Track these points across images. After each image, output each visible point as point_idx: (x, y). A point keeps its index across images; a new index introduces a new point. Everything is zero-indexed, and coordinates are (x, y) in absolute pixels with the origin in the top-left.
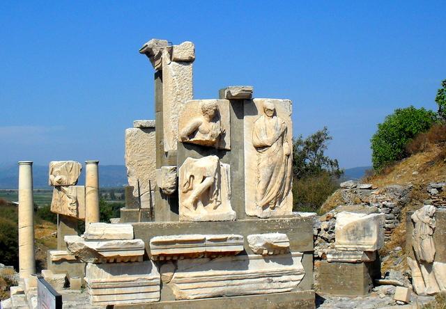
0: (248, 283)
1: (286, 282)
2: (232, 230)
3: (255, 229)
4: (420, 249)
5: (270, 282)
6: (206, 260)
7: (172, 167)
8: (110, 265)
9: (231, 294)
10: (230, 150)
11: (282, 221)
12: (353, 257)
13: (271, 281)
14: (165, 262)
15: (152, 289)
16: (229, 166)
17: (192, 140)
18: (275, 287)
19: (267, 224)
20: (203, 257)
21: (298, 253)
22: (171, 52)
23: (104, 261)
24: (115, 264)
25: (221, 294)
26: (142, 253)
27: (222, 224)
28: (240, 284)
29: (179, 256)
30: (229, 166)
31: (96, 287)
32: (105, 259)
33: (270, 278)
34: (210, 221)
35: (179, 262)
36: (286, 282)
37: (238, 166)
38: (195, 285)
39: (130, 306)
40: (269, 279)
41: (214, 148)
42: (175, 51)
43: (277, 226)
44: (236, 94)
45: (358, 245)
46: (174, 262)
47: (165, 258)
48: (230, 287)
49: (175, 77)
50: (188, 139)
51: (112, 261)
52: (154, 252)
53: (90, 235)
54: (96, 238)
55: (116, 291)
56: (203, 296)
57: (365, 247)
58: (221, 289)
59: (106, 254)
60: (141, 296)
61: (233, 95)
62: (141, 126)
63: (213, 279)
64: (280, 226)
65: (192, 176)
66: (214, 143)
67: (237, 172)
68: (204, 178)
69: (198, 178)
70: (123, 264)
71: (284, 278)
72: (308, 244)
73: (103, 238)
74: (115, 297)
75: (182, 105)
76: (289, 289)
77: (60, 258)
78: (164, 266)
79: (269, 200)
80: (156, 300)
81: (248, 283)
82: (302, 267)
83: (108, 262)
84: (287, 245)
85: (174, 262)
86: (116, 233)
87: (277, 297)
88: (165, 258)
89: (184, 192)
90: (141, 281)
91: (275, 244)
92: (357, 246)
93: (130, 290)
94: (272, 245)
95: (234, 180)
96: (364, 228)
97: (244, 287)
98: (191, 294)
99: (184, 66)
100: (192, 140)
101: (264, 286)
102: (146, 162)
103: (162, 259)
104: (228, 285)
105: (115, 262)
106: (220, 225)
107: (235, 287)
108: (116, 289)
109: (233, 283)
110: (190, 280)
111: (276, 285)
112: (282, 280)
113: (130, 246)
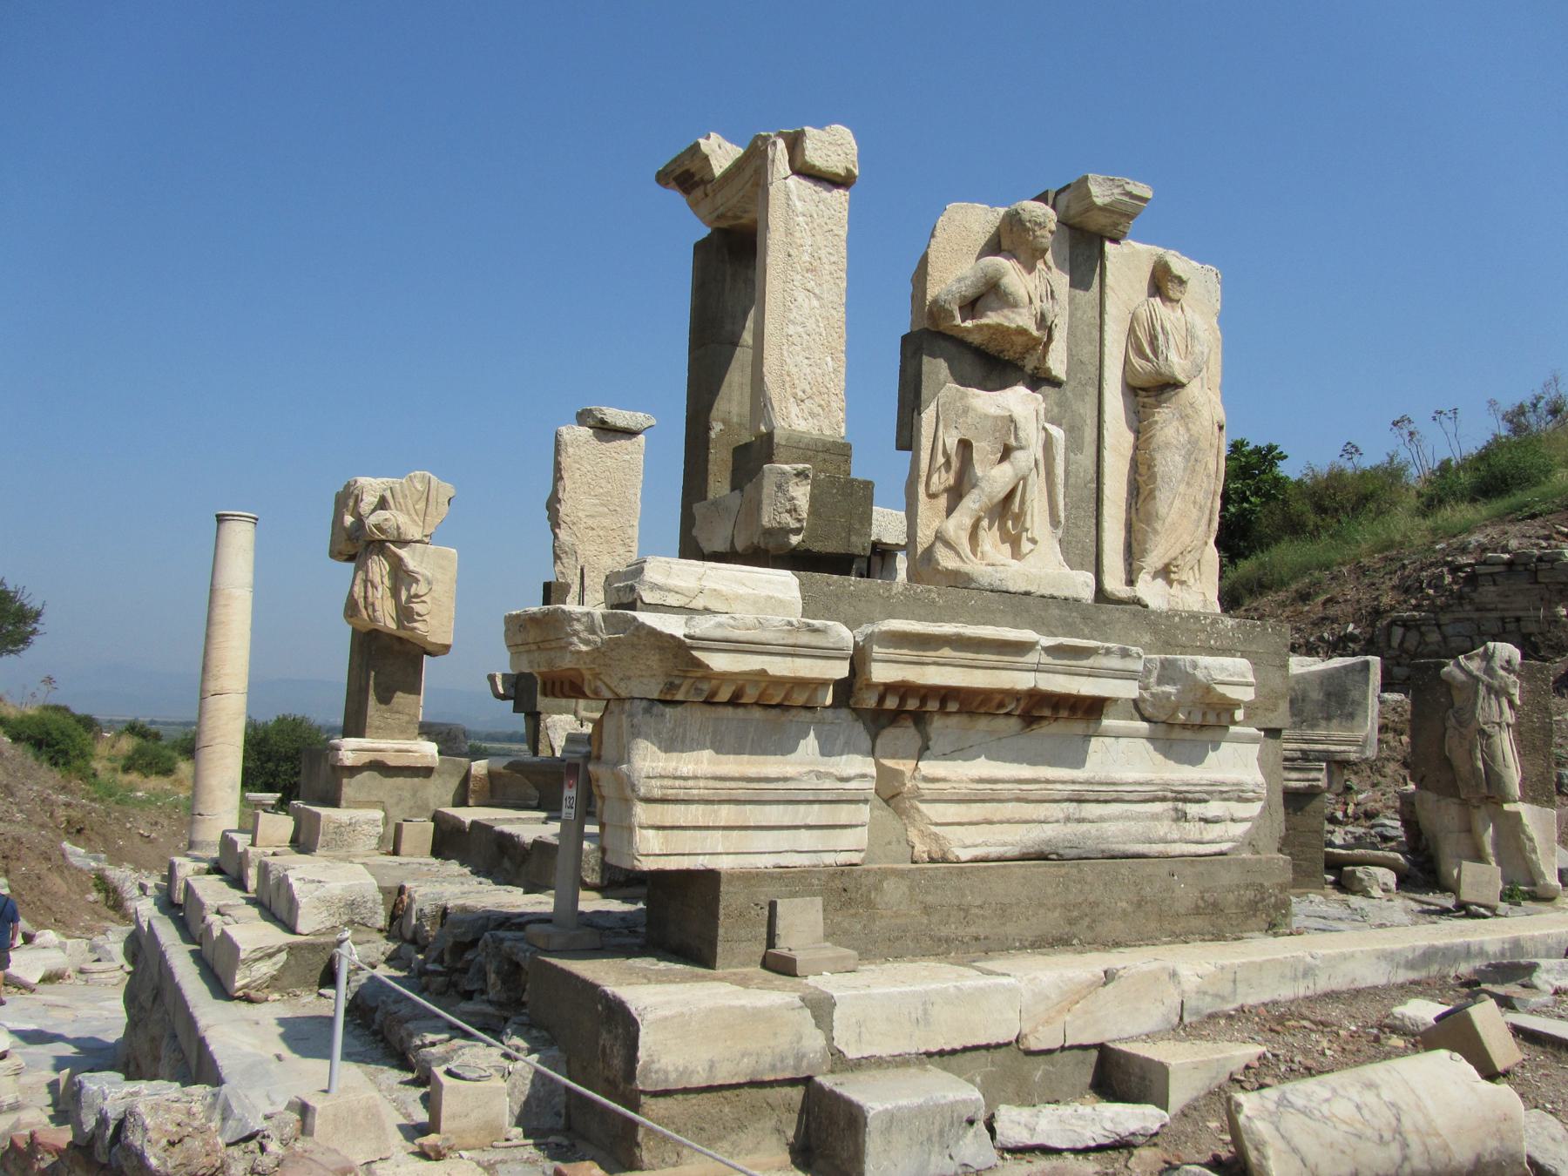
0: (1117, 818)
1: (1216, 821)
2: (1086, 631)
3: (1147, 638)
4: (1480, 765)
5: (1177, 820)
6: (1014, 723)
7: (800, 466)
8: (710, 712)
9: (1074, 852)
12: (1294, 775)
13: (1183, 817)
14: (895, 717)
15: (844, 814)
17: (969, 324)
18: (1182, 839)
20: (1008, 714)
21: (1253, 731)
22: (795, 143)
23: (698, 691)
24: (730, 711)
25: (1047, 849)
26: (841, 670)
27: (1059, 607)
28: (1102, 819)
29: (946, 695)
31: (657, 793)
32: (706, 687)
33: (1180, 805)
34: (1027, 594)
35: (937, 723)
36: (1216, 821)
37: (1082, 438)
38: (977, 811)
39: (771, 876)
40: (1176, 810)
41: (1021, 369)
42: (809, 145)
43: (1203, 636)
44: (1107, 200)
45: (1307, 742)
46: (919, 719)
47: (903, 700)
48: (1073, 828)
49: (801, 219)
50: (958, 321)
51: (724, 695)
52: (882, 673)
53: (655, 587)
54: (672, 600)
55: (726, 814)
56: (994, 851)
57: (1333, 748)
58: (1049, 832)
59: (719, 662)
60: (807, 839)
61: (1099, 201)
62: (603, 422)
63: (1032, 796)
64: (1209, 636)
65: (965, 446)
66: (1037, 341)
68: (1006, 453)
70: (757, 713)
71: (1214, 808)
72: (1276, 706)
73: (698, 603)
74: (716, 840)
75: (815, 303)
76: (1224, 847)
77: (366, 758)
78: (889, 735)
80: (855, 858)
81: (1117, 818)
82: (1260, 778)
83: (709, 702)
84: (1247, 695)
85: (919, 719)
86: (742, 591)
87: (1201, 868)
88: (903, 700)
90: (815, 783)
91: (1220, 689)
92: (1305, 746)
93: (774, 814)
94: (1208, 689)
95: (1072, 481)
96: (1328, 695)
97: (1111, 828)
98: (966, 843)
99: (825, 194)
101: (1164, 828)
102: (606, 522)
103: (891, 703)
104: (1068, 819)
105: (734, 702)
106: (1056, 612)
107: (1085, 826)
108: (725, 808)
109: (1083, 814)
110: (964, 790)
111: (1193, 829)
112: (1209, 815)
113: (805, 638)
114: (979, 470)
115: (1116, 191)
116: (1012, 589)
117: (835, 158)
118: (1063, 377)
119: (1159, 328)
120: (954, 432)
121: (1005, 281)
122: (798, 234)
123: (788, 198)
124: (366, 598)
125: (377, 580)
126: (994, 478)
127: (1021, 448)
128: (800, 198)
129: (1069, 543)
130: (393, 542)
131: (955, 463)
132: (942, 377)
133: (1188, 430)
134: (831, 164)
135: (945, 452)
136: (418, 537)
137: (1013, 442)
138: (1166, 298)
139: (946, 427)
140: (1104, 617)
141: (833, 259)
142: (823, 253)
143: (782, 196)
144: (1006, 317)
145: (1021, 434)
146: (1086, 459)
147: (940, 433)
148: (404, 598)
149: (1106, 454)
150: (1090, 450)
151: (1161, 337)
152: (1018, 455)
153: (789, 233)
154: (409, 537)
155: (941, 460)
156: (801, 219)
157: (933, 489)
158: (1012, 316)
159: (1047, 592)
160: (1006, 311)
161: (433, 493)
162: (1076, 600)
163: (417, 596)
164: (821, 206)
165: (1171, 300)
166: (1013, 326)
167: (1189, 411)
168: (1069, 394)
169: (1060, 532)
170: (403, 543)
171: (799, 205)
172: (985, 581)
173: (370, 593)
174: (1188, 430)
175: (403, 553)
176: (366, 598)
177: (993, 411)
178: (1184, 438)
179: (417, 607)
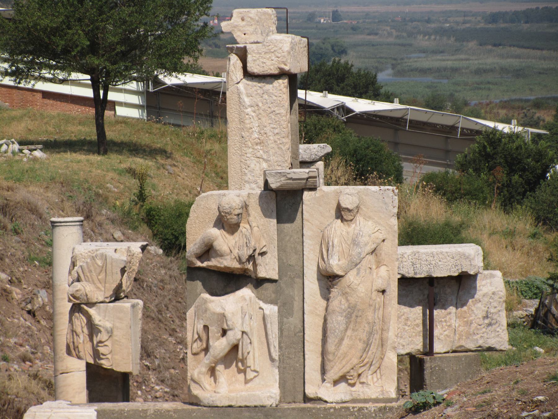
10: (274, 281)
11: (360, 409)
16: (276, 308)
19: (332, 414)
30: (276, 308)
34: (230, 406)
42: (249, 58)
44: (278, 184)
49: (249, 110)
67: (291, 319)
68: (224, 332)
69: (214, 330)
79: (345, 370)
89: (195, 354)
95: (285, 333)
100: (205, 264)
106: (247, 414)
114: (211, 343)
115: (283, 179)
116: (219, 405)
117: (269, 63)
118: (276, 277)
119: (331, 244)
120: (201, 322)
121: (216, 244)
122: (247, 121)
123: (240, 98)
124: (73, 342)
125: (79, 330)
126: (220, 346)
127: (230, 330)
128: (248, 95)
129: (285, 368)
130: (86, 304)
131: (204, 337)
132: (198, 291)
133: (348, 300)
134: (266, 68)
135: (198, 334)
136: (101, 299)
137: (225, 327)
138: (343, 220)
139: (198, 319)
140: (278, 414)
141: (276, 131)
142: (267, 130)
143: (235, 97)
144: (218, 261)
145: (229, 323)
146: (294, 321)
147: (196, 322)
148: (95, 343)
149: (305, 316)
150: (298, 314)
151: (330, 249)
152: (229, 333)
153: (242, 121)
154: (95, 300)
155: (196, 336)
156: (249, 110)
157: (194, 351)
158: (221, 261)
159: (243, 404)
160: (218, 259)
161: (109, 266)
162: (262, 406)
163: (100, 342)
164: (266, 96)
165: (347, 221)
166: (222, 266)
167: (348, 290)
168: (282, 285)
169: (277, 364)
170: (91, 304)
171: (247, 100)
172: (206, 402)
173: (75, 341)
174: (348, 300)
175: (92, 311)
176: (73, 342)
177: (218, 310)
178: (345, 305)
179: (102, 350)
